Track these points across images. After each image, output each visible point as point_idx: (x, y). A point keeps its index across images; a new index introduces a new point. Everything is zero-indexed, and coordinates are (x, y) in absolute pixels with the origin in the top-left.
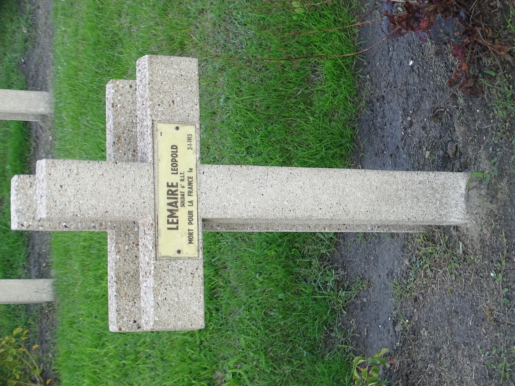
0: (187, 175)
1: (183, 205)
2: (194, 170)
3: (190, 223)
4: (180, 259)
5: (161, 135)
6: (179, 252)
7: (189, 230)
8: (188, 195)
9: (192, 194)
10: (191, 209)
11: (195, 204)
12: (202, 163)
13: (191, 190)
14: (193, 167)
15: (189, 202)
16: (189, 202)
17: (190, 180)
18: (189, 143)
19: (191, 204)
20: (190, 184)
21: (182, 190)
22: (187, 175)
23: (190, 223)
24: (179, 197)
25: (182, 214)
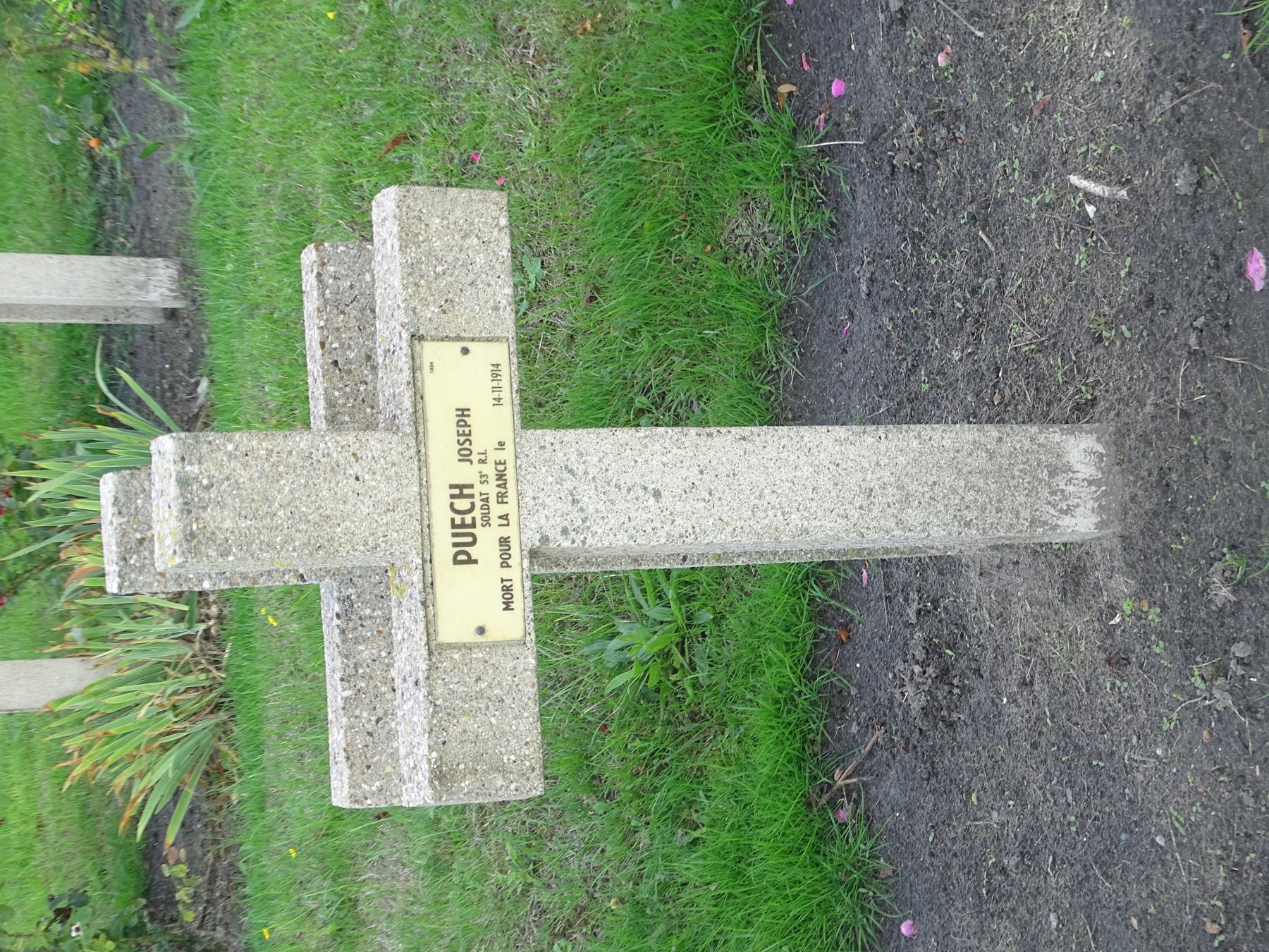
0: (493, 456)
2: (509, 446)
3: (505, 564)
7: (503, 580)
10: (505, 532)
11: (513, 519)
13: (503, 491)
14: (508, 438)
15: (500, 517)
16: (500, 517)
17: (501, 467)
20: (501, 476)
21: (484, 488)
22: (493, 456)
23: (505, 564)
24: (478, 504)
25: (486, 545)
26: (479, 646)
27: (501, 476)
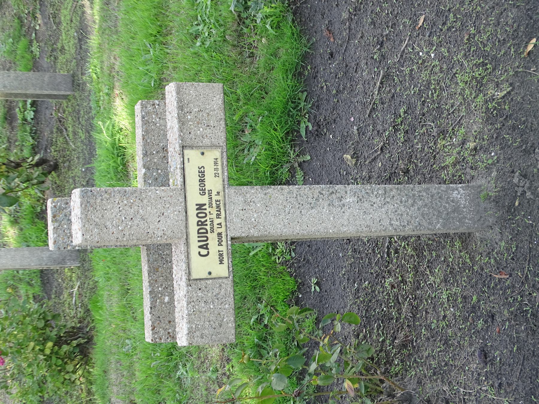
2: (222, 193)
3: (220, 244)
4: (211, 279)
7: (219, 251)
10: (220, 230)
11: (223, 224)
12: (230, 185)
15: (218, 224)
16: (218, 224)
18: (216, 167)
20: (218, 207)
22: (214, 198)
27: (218, 207)
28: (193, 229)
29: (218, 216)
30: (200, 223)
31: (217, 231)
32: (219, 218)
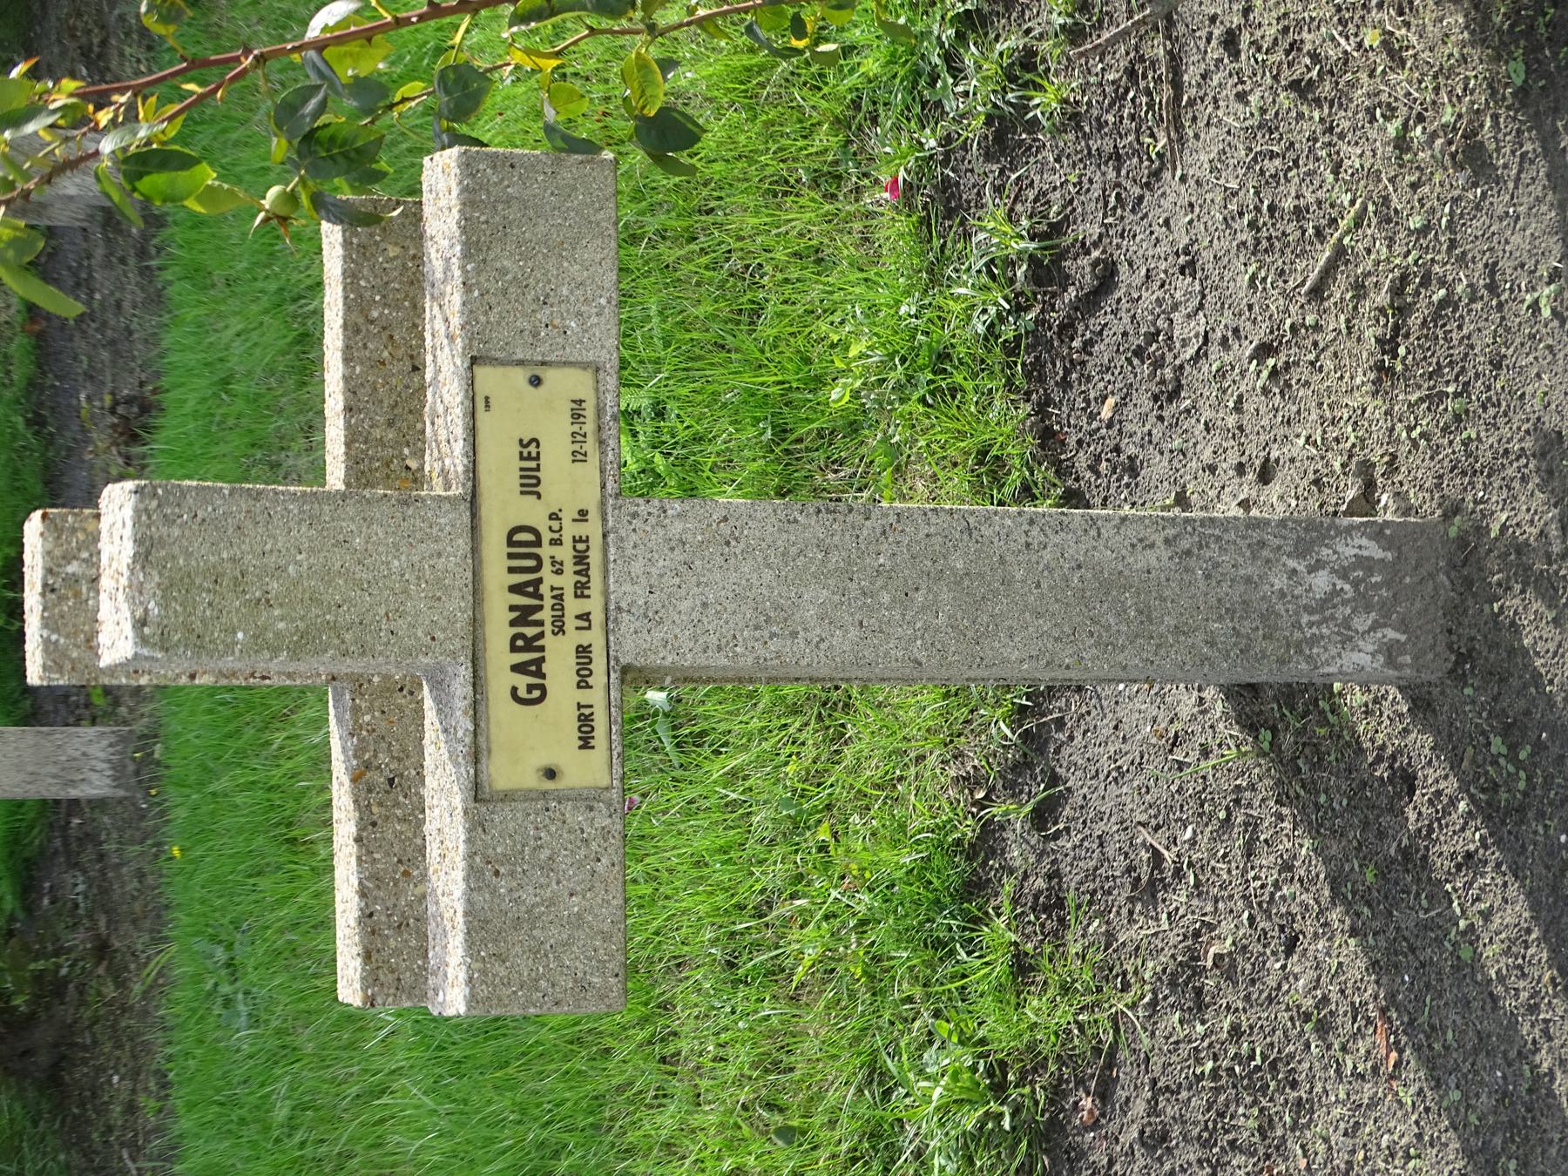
1: (560, 630)
2: (594, 516)
3: (583, 684)
5: (487, 405)
6: (551, 774)
7: (580, 706)
8: (576, 596)
9: (586, 592)
10: (585, 638)
11: (597, 618)
13: (584, 579)
15: (577, 617)
16: (577, 617)
17: (581, 547)
18: (576, 428)
19: (586, 624)
20: (581, 559)
21: (557, 581)
22: (570, 530)
23: (583, 684)
24: (548, 602)
25: (559, 656)
26: (544, 794)
27: (581, 559)
28: (499, 631)
29: (581, 590)
30: (520, 643)
31: (573, 638)
32: (583, 596)
